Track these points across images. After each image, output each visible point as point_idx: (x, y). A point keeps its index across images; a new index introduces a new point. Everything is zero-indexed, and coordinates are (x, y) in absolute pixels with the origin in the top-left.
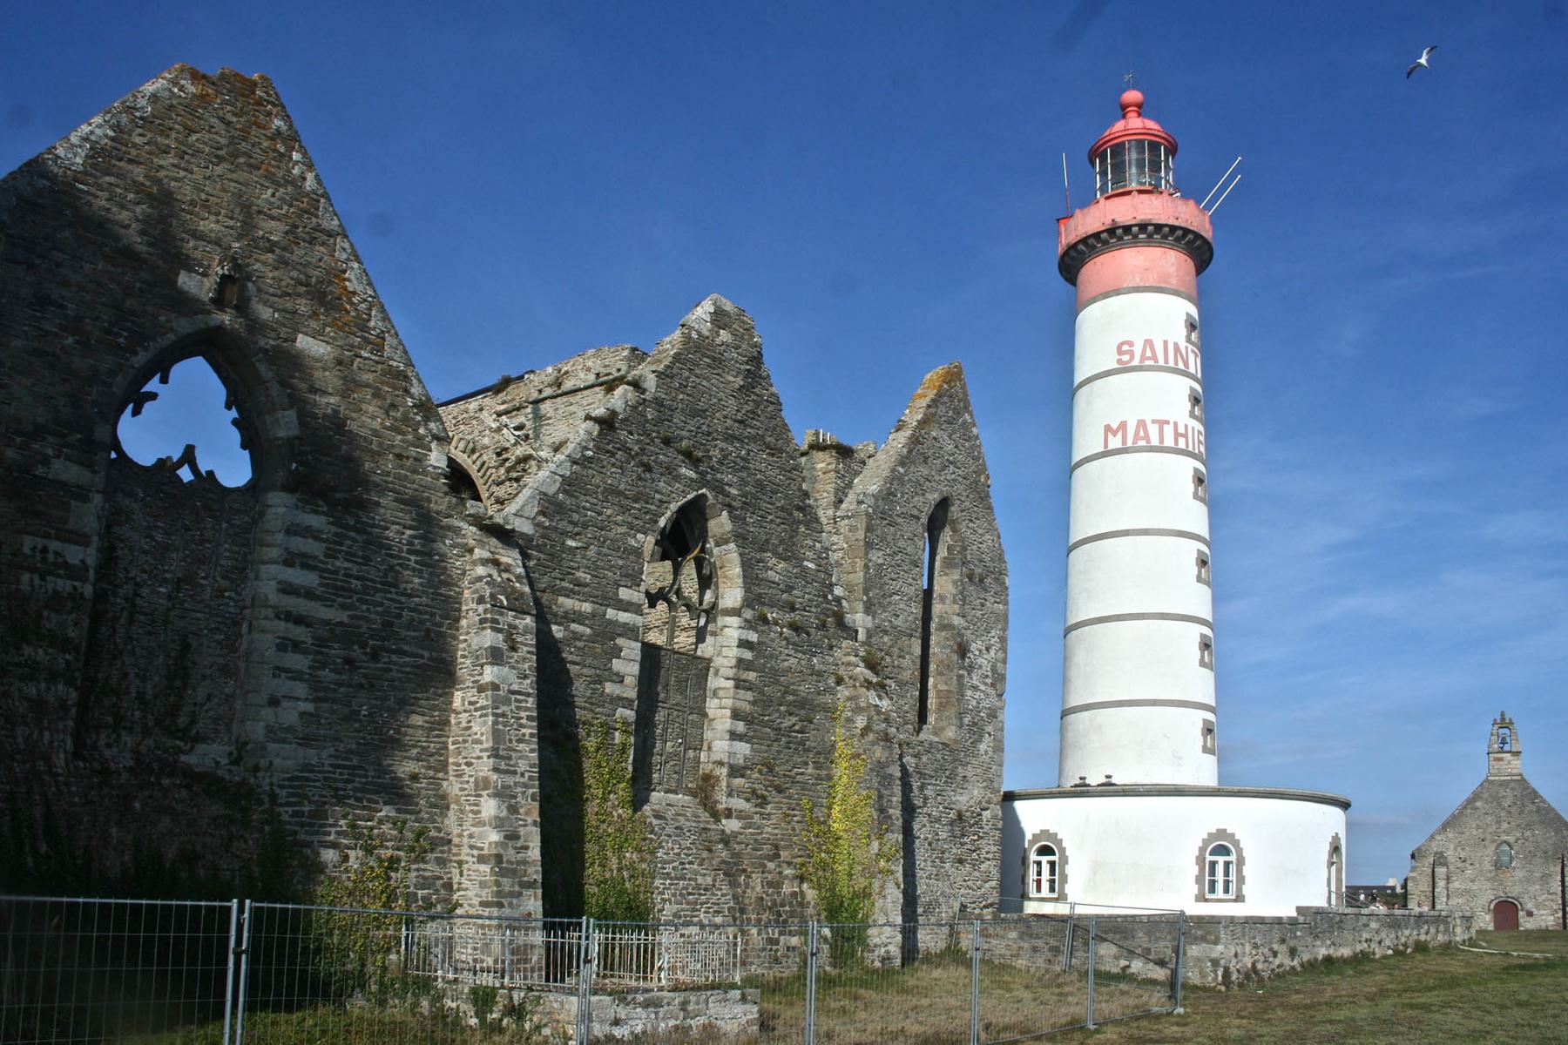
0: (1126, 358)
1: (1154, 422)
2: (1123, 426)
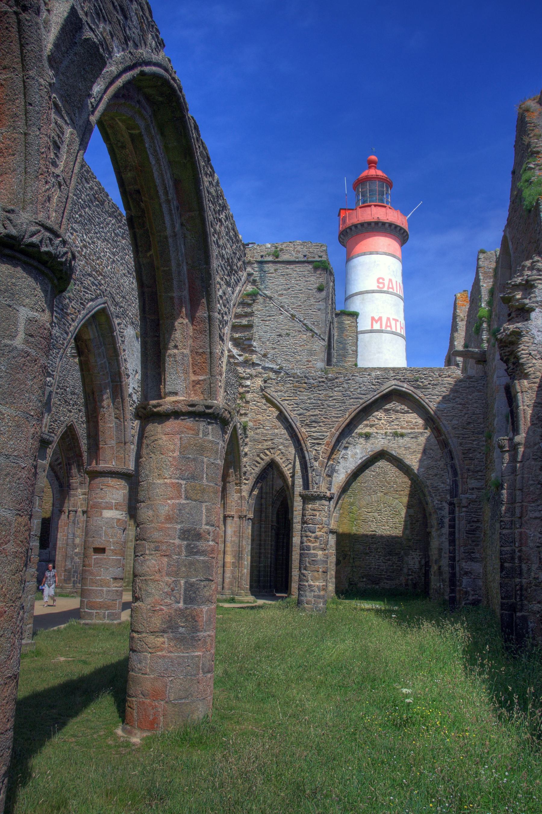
0: (381, 286)
1: (394, 319)
2: (380, 319)
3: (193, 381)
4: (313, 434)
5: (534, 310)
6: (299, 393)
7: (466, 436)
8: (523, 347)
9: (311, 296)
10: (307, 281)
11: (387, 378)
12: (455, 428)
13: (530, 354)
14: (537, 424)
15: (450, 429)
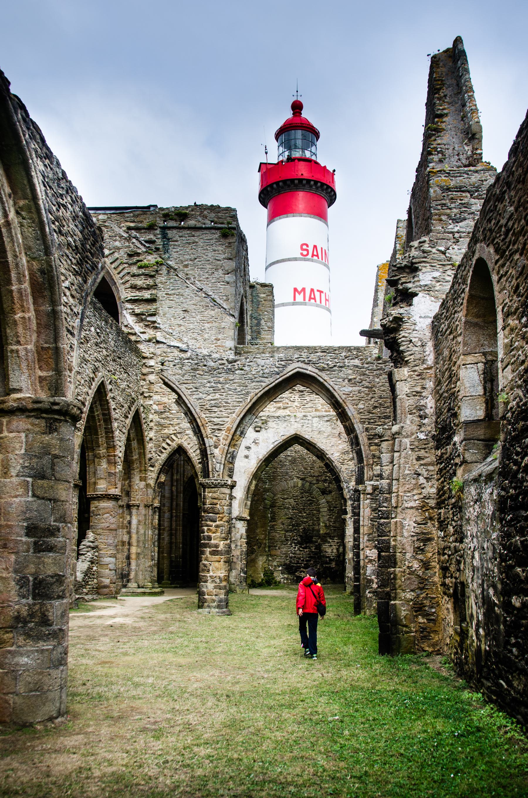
0: (305, 253)
1: (318, 291)
2: (304, 290)
3: (40, 377)
4: (212, 419)
5: (416, 295)
6: (198, 376)
7: (372, 421)
8: (403, 334)
9: (219, 267)
10: (215, 251)
11: (290, 360)
12: (361, 413)
13: (411, 341)
14: (415, 413)
15: (355, 413)
